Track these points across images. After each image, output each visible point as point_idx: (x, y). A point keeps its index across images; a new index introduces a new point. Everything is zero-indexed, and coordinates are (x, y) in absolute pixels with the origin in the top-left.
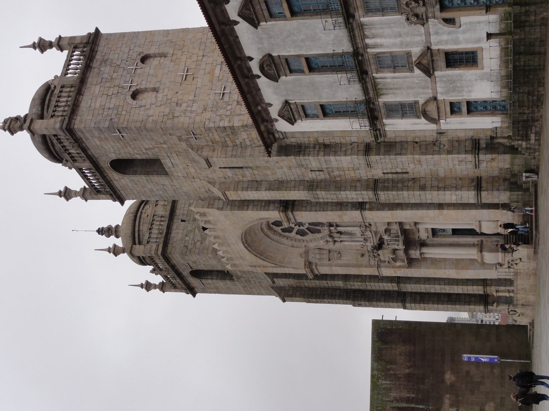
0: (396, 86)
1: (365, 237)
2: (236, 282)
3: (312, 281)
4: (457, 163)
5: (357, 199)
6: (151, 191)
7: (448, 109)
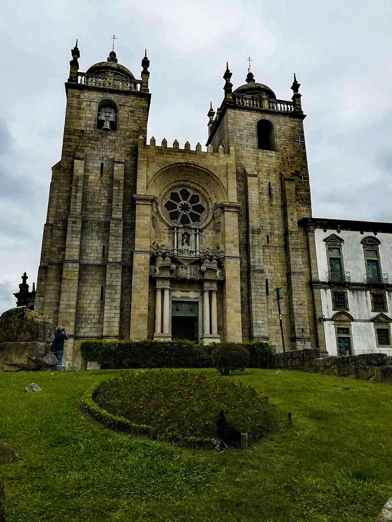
0: (360, 301)
1: (184, 252)
2: (92, 129)
3: (122, 195)
4: (301, 327)
5: (254, 258)
6: (242, 130)
7: (343, 327)
